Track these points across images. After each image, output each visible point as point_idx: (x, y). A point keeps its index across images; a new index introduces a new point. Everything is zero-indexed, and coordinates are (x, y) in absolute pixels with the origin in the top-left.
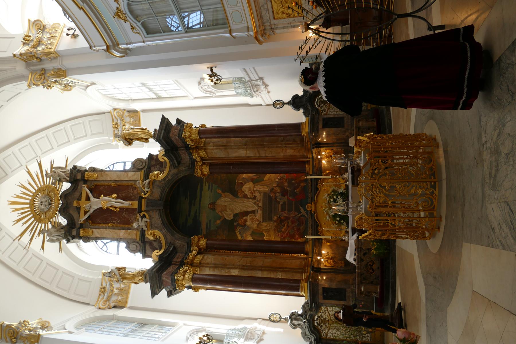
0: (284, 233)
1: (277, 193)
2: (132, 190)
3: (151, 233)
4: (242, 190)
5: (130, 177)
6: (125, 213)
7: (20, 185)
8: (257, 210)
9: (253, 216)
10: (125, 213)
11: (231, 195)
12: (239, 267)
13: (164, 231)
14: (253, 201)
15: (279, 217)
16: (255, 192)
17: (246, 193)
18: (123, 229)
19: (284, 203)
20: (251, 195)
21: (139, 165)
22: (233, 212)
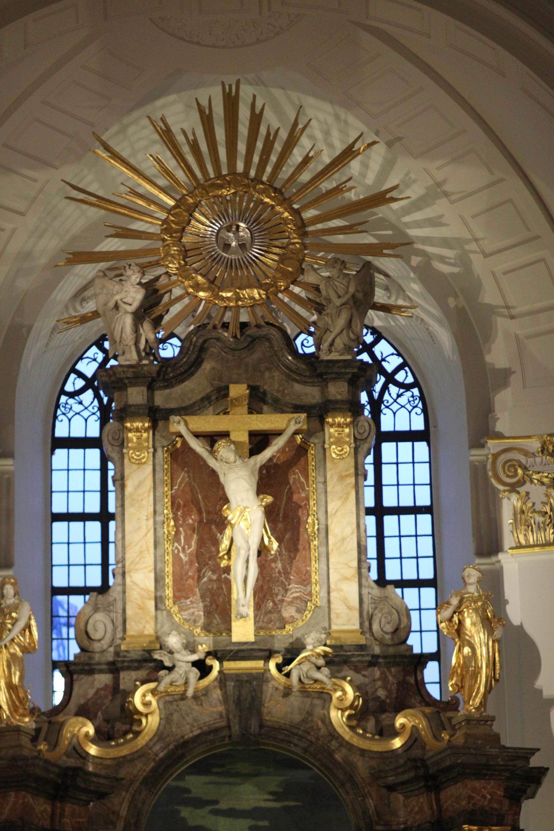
2: (297, 598)
3: (147, 704)
5: (339, 590)
6: (214, 577)
7: (300, 126)
10: (214, 577)
13: (157, 747)
18: (158, 580)
21: (383, 623)
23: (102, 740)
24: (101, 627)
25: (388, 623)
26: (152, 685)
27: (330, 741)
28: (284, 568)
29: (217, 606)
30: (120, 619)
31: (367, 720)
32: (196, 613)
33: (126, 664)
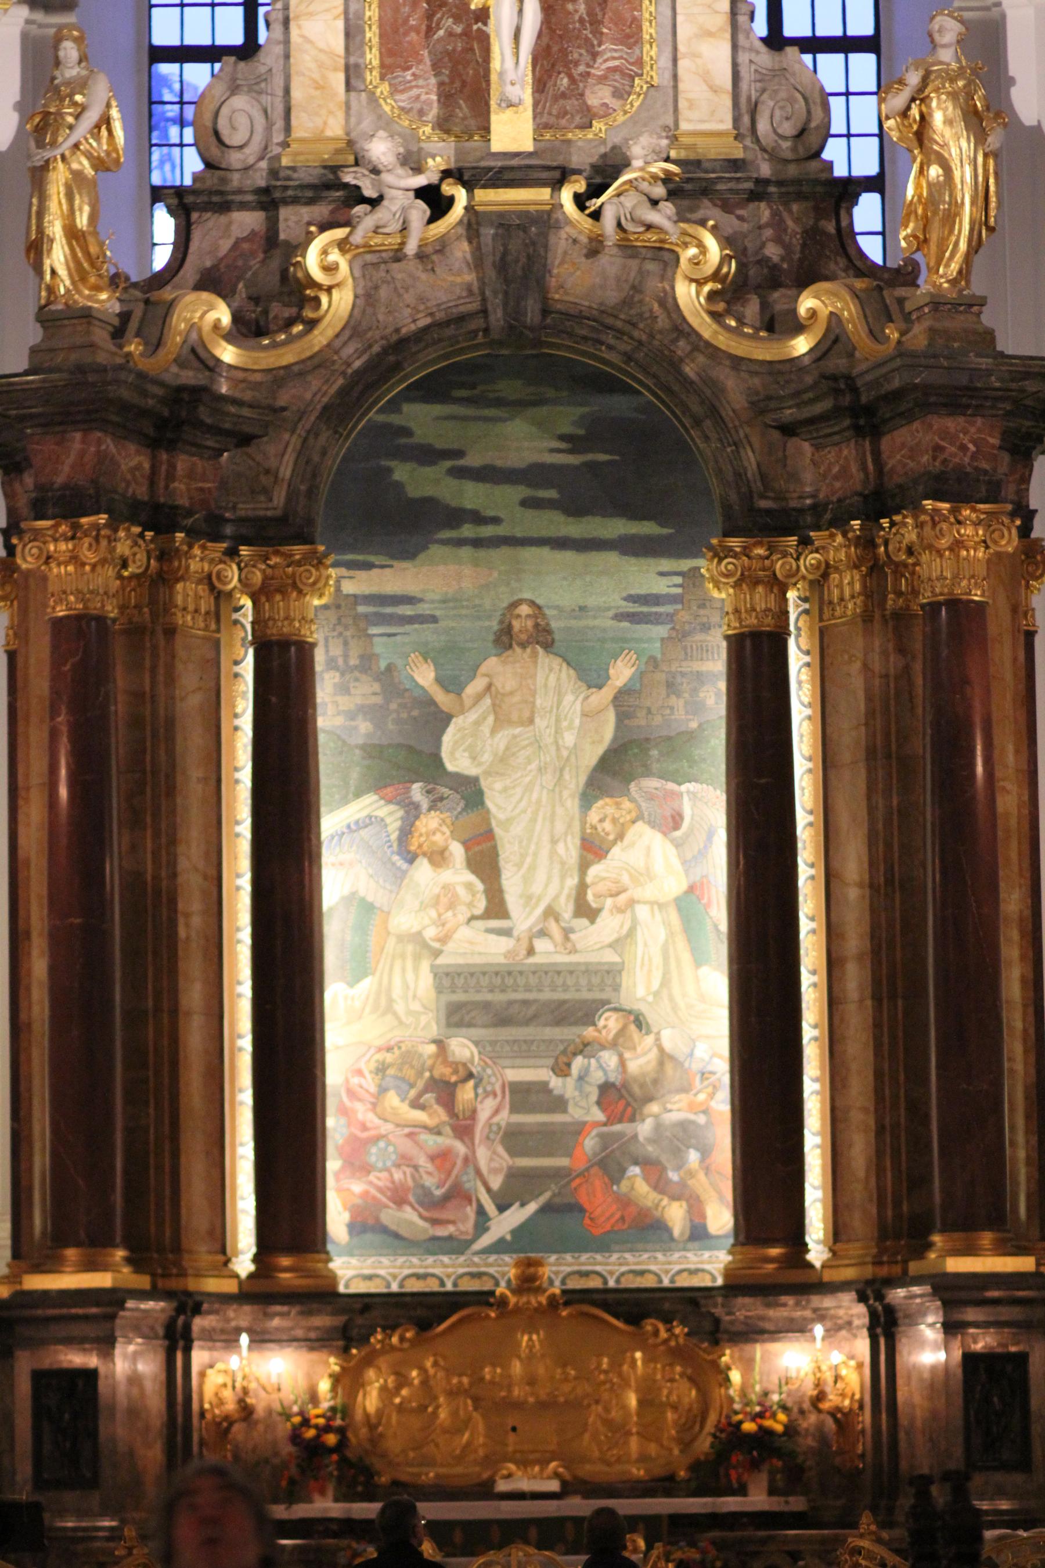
0: (375, 1103)
1: (621, 1056)
2: (614, 70)
3: (330, 269)
4: (634, 822)
5: (695, 55)
8: (507, 933)
9: (470, 905)
10: (458, 29)
11: (600, 750)
12: (163, 874)
13: (349, 350)
14: (562, 900)
15: (470, 1076)
16: (621, 911)
17: (616, 851)
18: (352, 33)
19: (559, 1104)
20: (601, 888)
22: (488, 773)
23: (246, 336)
24: (242, 122)
25: (787, 119)
26: (340, 233)
27: (675, 341)
28: (590, 13)
29: (464, 83)
30: (280, 108)
31: (745, 302)
32: (423, 97)
33: (290, 193)
